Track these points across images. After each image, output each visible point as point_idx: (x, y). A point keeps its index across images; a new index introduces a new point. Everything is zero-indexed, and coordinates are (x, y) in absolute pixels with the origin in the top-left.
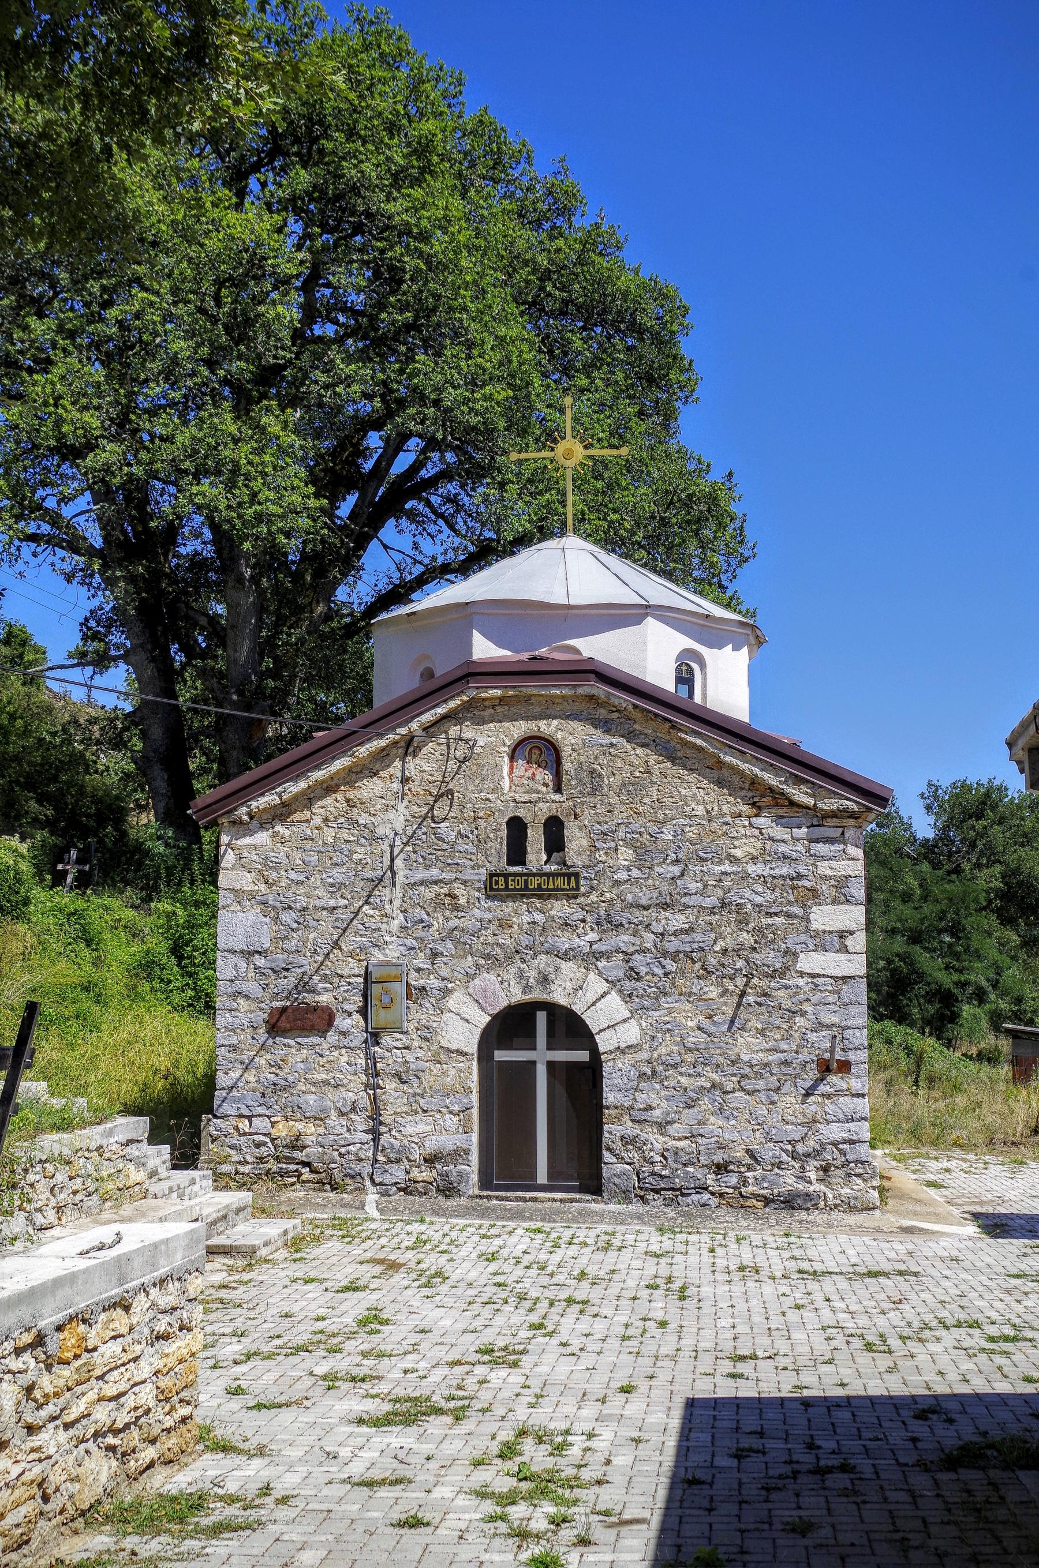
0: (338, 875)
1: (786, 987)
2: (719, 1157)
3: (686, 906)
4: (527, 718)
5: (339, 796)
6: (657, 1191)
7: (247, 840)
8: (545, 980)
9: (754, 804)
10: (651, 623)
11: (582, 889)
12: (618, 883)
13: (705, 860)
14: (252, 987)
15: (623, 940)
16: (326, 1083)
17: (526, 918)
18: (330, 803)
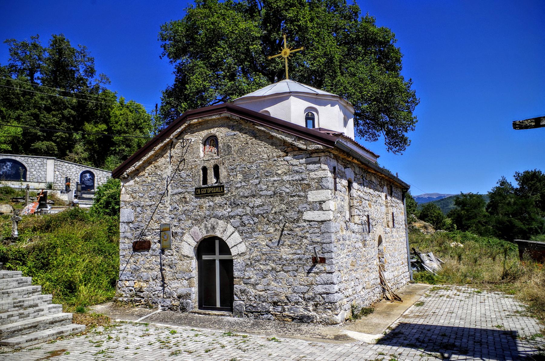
0: (153, 193)
1: (299, 227)
2: (275, 299)
3: (261, 196)
4: (207, 129)
5: (152, 165)
6: (252, 313)
7: (127, 184)
8: (213, 228)
9: (285, 152)
10: (293, 99)
11: (225, 192)
12: (237, 188)
13: (267, 176)
14: (129, 234)
15: (239, 210)
16: (149, 268)
17: (208, 205)
18: (149, 169)
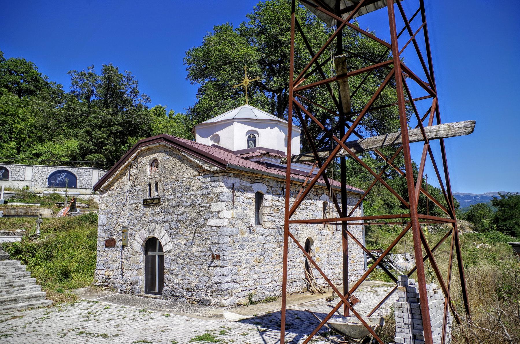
0: (118, 203)
1: (205, 231)
2: (189, 286)
3: (183, 206)
4: (152, 154)
5: (118, 182)
6: (174, 296)
7: (103, 196)
8: (153, 231)
9: (198, 172)
10: (236, 124)
11: (161, 203)
12: (168, 200)
13: (187, 191)
14: (103, 235)
15: (169, 217)
16: (114, 261)
17: (151, 212)
18: (117, 184)
